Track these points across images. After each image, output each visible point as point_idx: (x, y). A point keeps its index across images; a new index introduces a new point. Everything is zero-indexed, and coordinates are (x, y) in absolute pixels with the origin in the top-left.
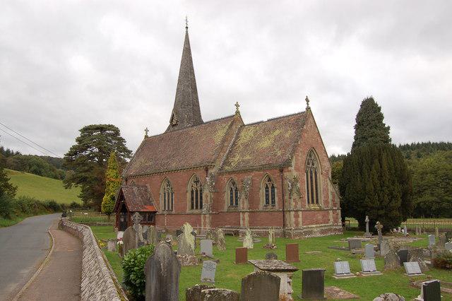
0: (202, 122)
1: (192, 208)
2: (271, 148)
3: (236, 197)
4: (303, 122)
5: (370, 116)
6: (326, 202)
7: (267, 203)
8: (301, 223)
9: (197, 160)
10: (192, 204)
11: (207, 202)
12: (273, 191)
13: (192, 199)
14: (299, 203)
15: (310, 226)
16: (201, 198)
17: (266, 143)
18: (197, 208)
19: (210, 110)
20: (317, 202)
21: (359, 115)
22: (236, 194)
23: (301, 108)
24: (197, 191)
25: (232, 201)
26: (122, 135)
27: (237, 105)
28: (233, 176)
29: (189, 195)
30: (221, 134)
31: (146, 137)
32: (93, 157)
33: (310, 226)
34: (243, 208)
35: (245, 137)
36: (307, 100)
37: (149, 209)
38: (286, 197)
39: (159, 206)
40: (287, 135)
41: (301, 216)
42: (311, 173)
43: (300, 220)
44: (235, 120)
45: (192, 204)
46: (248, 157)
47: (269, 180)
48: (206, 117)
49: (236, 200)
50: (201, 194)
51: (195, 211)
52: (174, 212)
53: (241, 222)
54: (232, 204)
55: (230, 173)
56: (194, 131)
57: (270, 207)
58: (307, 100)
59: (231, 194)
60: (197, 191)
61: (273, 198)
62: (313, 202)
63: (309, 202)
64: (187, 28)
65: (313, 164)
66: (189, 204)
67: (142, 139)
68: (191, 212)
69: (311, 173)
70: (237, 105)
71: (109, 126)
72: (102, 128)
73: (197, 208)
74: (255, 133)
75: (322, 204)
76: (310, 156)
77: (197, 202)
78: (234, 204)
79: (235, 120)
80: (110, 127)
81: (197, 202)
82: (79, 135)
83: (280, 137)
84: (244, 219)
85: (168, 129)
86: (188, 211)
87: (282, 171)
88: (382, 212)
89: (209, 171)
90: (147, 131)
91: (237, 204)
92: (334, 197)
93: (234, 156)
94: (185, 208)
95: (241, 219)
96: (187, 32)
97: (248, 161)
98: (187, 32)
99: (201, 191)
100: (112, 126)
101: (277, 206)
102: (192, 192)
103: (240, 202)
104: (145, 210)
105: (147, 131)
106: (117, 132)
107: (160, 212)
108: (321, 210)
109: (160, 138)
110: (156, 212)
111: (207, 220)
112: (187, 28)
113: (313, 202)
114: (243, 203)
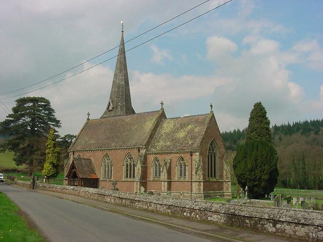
0: (134, 112)
1: (127, 177)
2: (185, 138)
3: (160, 171)
5: (259, 114)
7: (181, 175)
9: (132, 142)
10: (127, 174)
11: (138, 173)
13: (127, 170)
15: (209, 192)
16: (134, 170)
17: (181, 134)
18: (130, 177)
20: (215, 176)
21: (252, 112)
23: (208, 111)
24: (130, 165)
26: (52, 106)
27: (162, 104)
29: (124, 168)
30: (149, 125)
31: (88, 119)
32: (26, 126)
33: (209, 192)
34: (164, 179)
35: (167, 127)
36: (211, 106)
37: (94, 177)
38: (194, 173)
39: (100, 174)
41: (202, 185)
43: (202, 187)
45: (127, 174)
46: (168, 143)
48: (138, 106)
49: (160, 173)
51: (129, 179)
54: (156, 175)
55: (155, 154)
56: (128, 119)
57: (182, 178)
58: (211, 106)
60: (130, 165)
61: (185, 173)
63: (208, 176)
64: (123, 31)
65: (213, 150)
66: (124, 174)
67: (85, 121)
68: (126, 180)
70: (162, 104)
71: (42, 98)
72: (34, 100)
73: (130, 177)
74: (174, 126)
77: (130, 173)
80: (42, 99)
81: (130, 173)
83: (192, 130)
84: (164, 186)
85: (105, 113)
86: (123, 180)
87: (191, 155)
89: (141, 152)
91: (160, 175)
92: (227, 173)
93: (159, 142)
96: (122, 35)
97: (169, 147)
98: (122, 35)
99: (134, 165)
100: (44, 99)
101: (187, 179)
102: (127, 165)
103: (162, 174)
104: (90, 177)
106: (48, 103)
107: (101, 179)
112: (123, 31)
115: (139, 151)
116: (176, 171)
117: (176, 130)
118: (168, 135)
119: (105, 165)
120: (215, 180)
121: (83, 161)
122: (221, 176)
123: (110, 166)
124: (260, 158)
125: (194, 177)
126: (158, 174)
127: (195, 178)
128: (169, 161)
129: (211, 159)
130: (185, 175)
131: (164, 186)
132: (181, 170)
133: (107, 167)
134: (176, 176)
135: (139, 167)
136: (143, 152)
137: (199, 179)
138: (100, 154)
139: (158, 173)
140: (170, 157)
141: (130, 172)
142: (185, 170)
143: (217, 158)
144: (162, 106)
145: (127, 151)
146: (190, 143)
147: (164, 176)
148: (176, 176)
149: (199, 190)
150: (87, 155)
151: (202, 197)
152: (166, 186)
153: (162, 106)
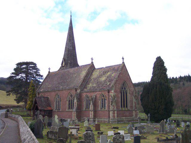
0: (78, 65)
1: (69, 109)
2: (105, 81)
4: (122, 70)
6: (132, 107)
7: (102, 107)
8: (116, 116)
9: (72, 85)
12: (105, 102)
13: (69, 104)
14: (115, 107)
15: (122, 118)
16: (73, 104)
17: (103, 79)
19: (82, 60)
20: (127, 107)
21: (155, 62)
22: (89, 102)
23: (120, 62)
24: (71, 100)
25: (87, 105)
26: (38, 66)
27: (92, 59)
28: (88, 94)
30: (84, 73)
31: (49, 72)
33: (122, 118)
34: (91, 109)
35: (95, 74)
36: (123, 59)
37: (49, 108)
38: (110, 105)
40: (113, 75)
41: (116, 113)
42: (124, 93)
43: (116, 115)
44: (92, 67)
46: (95, 85)
47: (104, 96)
49: (89, 105)
50: (73, 102)
51: (70, 110)
52: (61, 110)
53: (90, 115)
54: (87, 107)
57: (103, 109)
58: (123, 59)
59: (87, 102)
61: (105, 105)
62: (124, 107)
63: (122, 107)
64: (71, 16)
65: (125, 89)
67: (47, 73)
68: (69, 110)
69: (124, 93)
72: (27, 64)
75: (129, 108)
76: (124, 85)
77: (71, 105)
78: (88, 107)
79: (92, 67)
80: (32, 63)
81: (71, 105)
82: (15, 67)
83: (110, 75)
84: (91, 114)
85: (61, 68)
86: (67, 110)
87: (109, 92)
88: (156, 111)
89: (77, 91)
90: (49, 69)
91: (89, 107)
94: (66, 109)
95: (90, 114)
96: (71, 18)
98: (71, 18)
100: (33, 63)
102: (69, 101)
105: (49, 69)
106: (35, 64)
107: (54, 110)
108: (128, 110)
109: (55, 74)
110: (52, 110)
111: (75, 115)
112: (71, 16)
113: (124, 107)
114: (91, 107)
115: (76, 91)
116: (100, 103)
117: (100, 76)
118: (95, 79)
119: (57, 101)
120: (126, 109)
121: (43, 99)
122: (132, 107)
123: (59, 102)
124: (161, 95)
125: (111, 108)
126: (88, 106)
127: (111, 108)
128: (95, 97)
129: (124, 95)
130: (105, 107)
131: (91, 114)
132: (102, 103)
133: (58, 102)
134: (100, 107)
135: (75, 101)
136: (79, 91)
137: (114, 109)
138: (53, 94)
139: (88, 107)
140: (95, 95)
141: (71, 106)
142: (105, 103)
143: (128, 94)
144: (92, 61)
145: (69, 91)
146: (108, 84)
147: (91, 107)
148: (100, 107)
149: (114, 116)
150: (46, 95)
151: (116, 121)
152: (92, 114)
153: (92, 61)
